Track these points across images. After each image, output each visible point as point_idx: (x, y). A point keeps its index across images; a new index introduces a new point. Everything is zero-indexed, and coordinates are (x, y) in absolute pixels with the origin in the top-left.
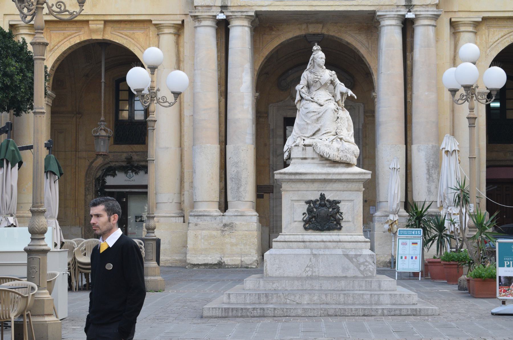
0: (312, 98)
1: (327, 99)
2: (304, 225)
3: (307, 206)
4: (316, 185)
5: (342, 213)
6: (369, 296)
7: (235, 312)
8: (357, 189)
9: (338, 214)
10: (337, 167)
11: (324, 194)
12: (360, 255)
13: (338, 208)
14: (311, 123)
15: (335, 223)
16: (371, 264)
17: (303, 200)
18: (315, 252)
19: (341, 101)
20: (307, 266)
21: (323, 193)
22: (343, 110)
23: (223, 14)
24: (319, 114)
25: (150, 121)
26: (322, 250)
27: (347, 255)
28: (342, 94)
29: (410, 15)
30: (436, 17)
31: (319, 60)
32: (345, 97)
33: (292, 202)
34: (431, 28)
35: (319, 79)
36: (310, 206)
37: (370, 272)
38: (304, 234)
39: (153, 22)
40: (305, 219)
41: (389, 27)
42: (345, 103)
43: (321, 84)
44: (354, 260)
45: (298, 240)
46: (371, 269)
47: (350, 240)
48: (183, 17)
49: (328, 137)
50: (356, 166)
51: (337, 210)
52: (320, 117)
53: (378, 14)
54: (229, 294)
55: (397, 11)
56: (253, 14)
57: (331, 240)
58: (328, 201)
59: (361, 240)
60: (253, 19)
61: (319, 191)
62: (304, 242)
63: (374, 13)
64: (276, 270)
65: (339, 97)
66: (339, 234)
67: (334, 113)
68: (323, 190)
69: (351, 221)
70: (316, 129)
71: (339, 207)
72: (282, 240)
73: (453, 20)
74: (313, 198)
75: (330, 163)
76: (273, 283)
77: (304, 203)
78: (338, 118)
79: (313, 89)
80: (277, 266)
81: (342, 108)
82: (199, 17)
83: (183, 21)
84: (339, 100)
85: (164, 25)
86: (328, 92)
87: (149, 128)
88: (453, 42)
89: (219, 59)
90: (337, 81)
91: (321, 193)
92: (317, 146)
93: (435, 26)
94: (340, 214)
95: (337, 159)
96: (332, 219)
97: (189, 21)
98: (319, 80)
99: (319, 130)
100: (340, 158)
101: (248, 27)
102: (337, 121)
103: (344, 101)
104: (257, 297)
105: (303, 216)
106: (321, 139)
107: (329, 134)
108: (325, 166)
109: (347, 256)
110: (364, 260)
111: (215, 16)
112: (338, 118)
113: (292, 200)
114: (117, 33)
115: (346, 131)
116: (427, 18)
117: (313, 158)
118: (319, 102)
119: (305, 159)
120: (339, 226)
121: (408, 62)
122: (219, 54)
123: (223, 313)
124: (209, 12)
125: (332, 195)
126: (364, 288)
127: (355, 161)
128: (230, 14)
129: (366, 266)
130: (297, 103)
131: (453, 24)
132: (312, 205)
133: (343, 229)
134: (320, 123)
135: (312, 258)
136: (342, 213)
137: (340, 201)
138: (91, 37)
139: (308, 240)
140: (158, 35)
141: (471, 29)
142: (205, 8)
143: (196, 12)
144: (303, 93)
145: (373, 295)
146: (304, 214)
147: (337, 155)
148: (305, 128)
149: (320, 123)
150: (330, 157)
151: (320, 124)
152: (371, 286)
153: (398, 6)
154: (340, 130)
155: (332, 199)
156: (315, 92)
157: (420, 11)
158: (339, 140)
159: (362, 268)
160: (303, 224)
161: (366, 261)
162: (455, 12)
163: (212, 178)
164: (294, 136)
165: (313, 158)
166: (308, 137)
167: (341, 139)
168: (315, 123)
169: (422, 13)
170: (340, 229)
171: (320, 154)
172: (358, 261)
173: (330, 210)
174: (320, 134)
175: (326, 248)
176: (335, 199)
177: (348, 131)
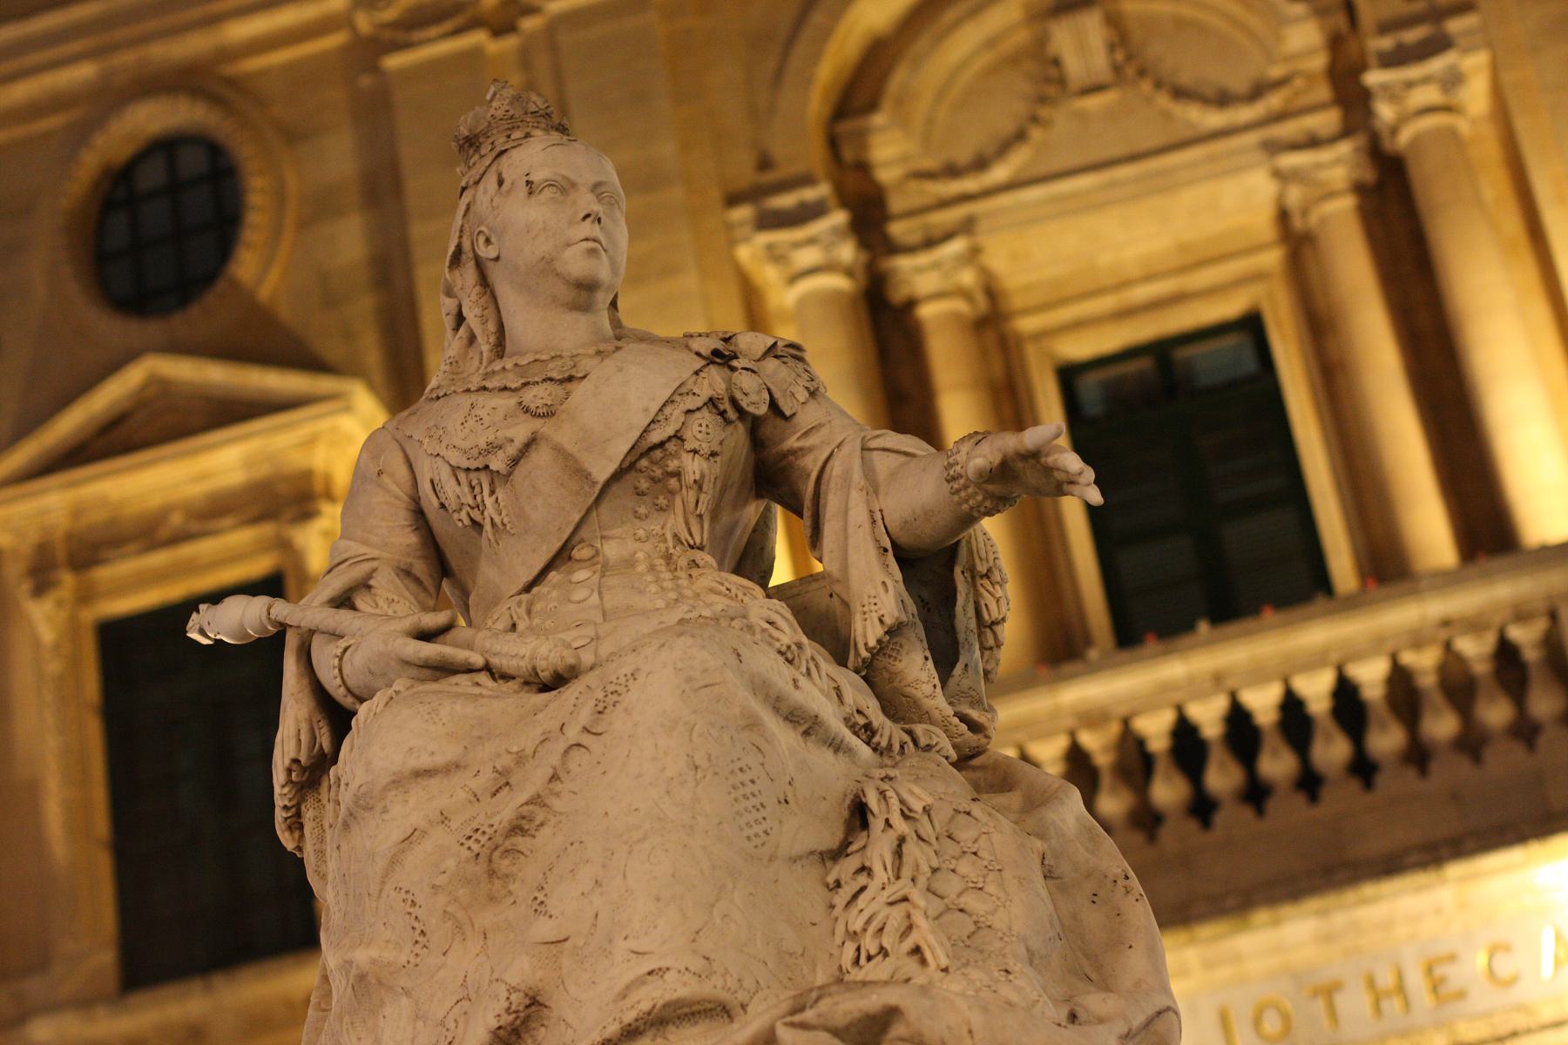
43: (584, 475)
134: (539, 908)
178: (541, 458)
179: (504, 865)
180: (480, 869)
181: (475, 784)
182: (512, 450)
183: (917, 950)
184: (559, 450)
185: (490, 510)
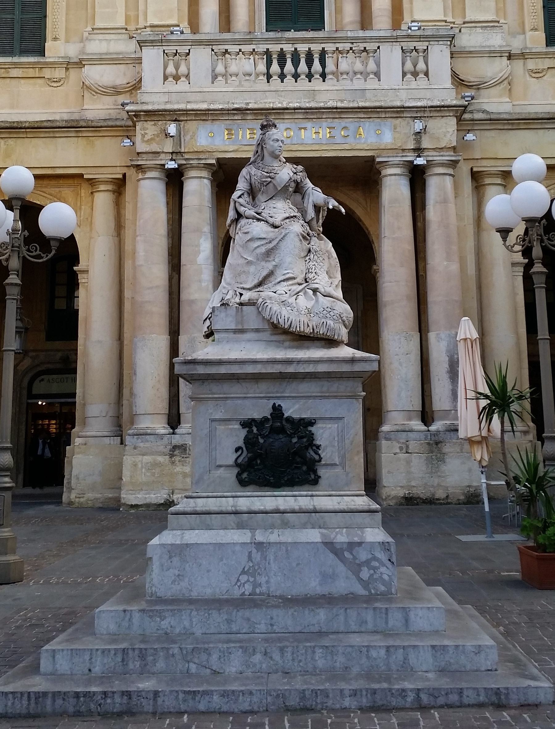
0: (258, 214)
1: (287, 215)
2: (238, 475)
3: (243, 433)
4: (264, 387)
5: (318, 447)
6: (383, 652)
7: (59, 702)
8: (350, 394)
9: (310, 448)
10: (308, 348)
11: (279, 405)
12: (360, 544)
13: (311, 436)
14: (255, 261)
15: (305, 468)
16: (384, 565)
17: (236, 420)
18: (260, 537)
19: (315, 220)
20: (243, 572)
21: (278, 402)
22: (320, 239)
23: (174, 162)
24: (270, 242)
25: (8, 284)
26: (276, 531)
27: (332, 543)
28: (317, 209)
29: (420, 161)
30: (454, 164)
31: (272, 143)
32: (323, 214)
33: (213, 423)
34: (448, 177)
35: (273, 178)
36: (250, 432)
37: (384, 583)
38: (239, 494)
39: (85, 177)
40: (239, 461)
41: (393, 177)
42: (323, 225)
44: (347, 554)
45: (224, 509)
46: (386, 577)
47: (337, 507)
48: (125, 170)
49: (290, 288)
50: (347, 345)
51: (307, 441)
52: (272, 249)
53: (378, 160)
54: (54, 651)
55: (403, 156)
56: (214, 162)
57: (297, 508)
58: (290, 420)
59: (360, 508)
60: (215, 168)
61: (269, 398)
62: (236, 513)
63: (373, 158)
64: (173, 582)
65: (311, 213)
66: (314, 493)
67: (301, 240)
68: (278, 398)
69: (338, 463)
70: (264, 273)
71: (313, 434)
72: (188, 509)
73: (475, 169)
74: (257, 415)
75: (294, 340)
76: (163, 618)
77: (237, 426)
78: (309, 251)
79: (261, 198)
80: (177, 573)
81: (318, 234)
82: (143, 167)
83: (124, 175)
84: (312, 219)
85: (100, 180)
86: (290, 204)
87: (7, 297)
88: (475, 199)
89: (171, 222)
90: (309, 184)
91: (274, 404)
92: (266, 304)
93: (453, 176)
94: (314, 448)
95: (308, 331)
96: (299, 460)
97: (131, 173)
98: (273, 180)
99: (271, 274)
100: (313, 330)
101: (208, 179)
102: (308, 257)
103: (321, 221)
104: (119, 659)
105: (235, 456)
106: (275, 292)
107: (290, 282)
108: (282, 345)
109: (329, 545)
110: (370, 556)
111: (164, 165)
112: (309, 251)
113: (213, 420)
114: (39, 192)
115: (327, 277)
116: (442, 165)
117: (257, 330)
118: (271, 220)
119: (242, 331)
120: (313, 476)
121: (419, 224)
122: (171, 216)
123: (33, 705)
124: (156, 160)
125: (297, 406)
126: (370, 626)
127: (343, 333)
128: (184, 162)
129: (375, 569)
130: (230, 226)
131: (476, 176)
132: (255, 430)
133: (321, 481)
134: (274, 260)
135: (254, 551)
136: (318, 447)
137: (313, 421)
138: (4, 197)
139: (245, 509)
140: (92, 193)
141: (499, 181)
142: (151, 155)
143: (138, 160)
144: (241, 205)
145: (392, 650)
146: (237, 450)
147: (306, 322)
148: (244, 272)
149: (274, 260)
150: (292, 326)
151: (274, 263)
152: (387, 623)
153: (403, 150)
154: (314, 274)
155: (296, 416)
156: (265, 203)
157: (433, 156)
158: (311, 292)
159: (365, 574)
160: (236, 471)
161: (375, 558)
162: (477, 159)
163: (159, 381)
164: (224, 288)
165: (257, 330)
166: (250, 289)
167: (315, 291)
168: (263, 260)
169: (435, 158)
170: (316, 482)
171: (271, 321)
172: (355, 558)
173: (295, 440)
174: (273, 283)
175: (286, 525)
176: (304, 416)
177: (330, 277)
178: (271, 184)
179: (270, 253)
180: (267, 253)
181: (267, 241)
182: (268, 182)
183: (315, 273)
184: (274, 184)
185: (262, 189)
